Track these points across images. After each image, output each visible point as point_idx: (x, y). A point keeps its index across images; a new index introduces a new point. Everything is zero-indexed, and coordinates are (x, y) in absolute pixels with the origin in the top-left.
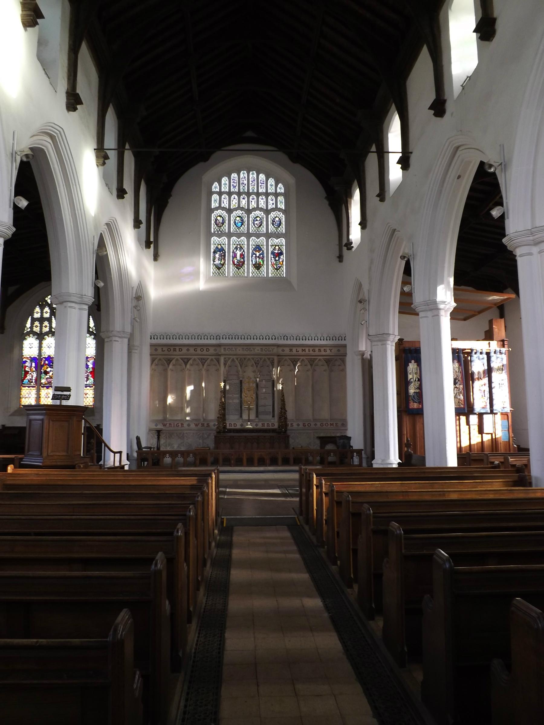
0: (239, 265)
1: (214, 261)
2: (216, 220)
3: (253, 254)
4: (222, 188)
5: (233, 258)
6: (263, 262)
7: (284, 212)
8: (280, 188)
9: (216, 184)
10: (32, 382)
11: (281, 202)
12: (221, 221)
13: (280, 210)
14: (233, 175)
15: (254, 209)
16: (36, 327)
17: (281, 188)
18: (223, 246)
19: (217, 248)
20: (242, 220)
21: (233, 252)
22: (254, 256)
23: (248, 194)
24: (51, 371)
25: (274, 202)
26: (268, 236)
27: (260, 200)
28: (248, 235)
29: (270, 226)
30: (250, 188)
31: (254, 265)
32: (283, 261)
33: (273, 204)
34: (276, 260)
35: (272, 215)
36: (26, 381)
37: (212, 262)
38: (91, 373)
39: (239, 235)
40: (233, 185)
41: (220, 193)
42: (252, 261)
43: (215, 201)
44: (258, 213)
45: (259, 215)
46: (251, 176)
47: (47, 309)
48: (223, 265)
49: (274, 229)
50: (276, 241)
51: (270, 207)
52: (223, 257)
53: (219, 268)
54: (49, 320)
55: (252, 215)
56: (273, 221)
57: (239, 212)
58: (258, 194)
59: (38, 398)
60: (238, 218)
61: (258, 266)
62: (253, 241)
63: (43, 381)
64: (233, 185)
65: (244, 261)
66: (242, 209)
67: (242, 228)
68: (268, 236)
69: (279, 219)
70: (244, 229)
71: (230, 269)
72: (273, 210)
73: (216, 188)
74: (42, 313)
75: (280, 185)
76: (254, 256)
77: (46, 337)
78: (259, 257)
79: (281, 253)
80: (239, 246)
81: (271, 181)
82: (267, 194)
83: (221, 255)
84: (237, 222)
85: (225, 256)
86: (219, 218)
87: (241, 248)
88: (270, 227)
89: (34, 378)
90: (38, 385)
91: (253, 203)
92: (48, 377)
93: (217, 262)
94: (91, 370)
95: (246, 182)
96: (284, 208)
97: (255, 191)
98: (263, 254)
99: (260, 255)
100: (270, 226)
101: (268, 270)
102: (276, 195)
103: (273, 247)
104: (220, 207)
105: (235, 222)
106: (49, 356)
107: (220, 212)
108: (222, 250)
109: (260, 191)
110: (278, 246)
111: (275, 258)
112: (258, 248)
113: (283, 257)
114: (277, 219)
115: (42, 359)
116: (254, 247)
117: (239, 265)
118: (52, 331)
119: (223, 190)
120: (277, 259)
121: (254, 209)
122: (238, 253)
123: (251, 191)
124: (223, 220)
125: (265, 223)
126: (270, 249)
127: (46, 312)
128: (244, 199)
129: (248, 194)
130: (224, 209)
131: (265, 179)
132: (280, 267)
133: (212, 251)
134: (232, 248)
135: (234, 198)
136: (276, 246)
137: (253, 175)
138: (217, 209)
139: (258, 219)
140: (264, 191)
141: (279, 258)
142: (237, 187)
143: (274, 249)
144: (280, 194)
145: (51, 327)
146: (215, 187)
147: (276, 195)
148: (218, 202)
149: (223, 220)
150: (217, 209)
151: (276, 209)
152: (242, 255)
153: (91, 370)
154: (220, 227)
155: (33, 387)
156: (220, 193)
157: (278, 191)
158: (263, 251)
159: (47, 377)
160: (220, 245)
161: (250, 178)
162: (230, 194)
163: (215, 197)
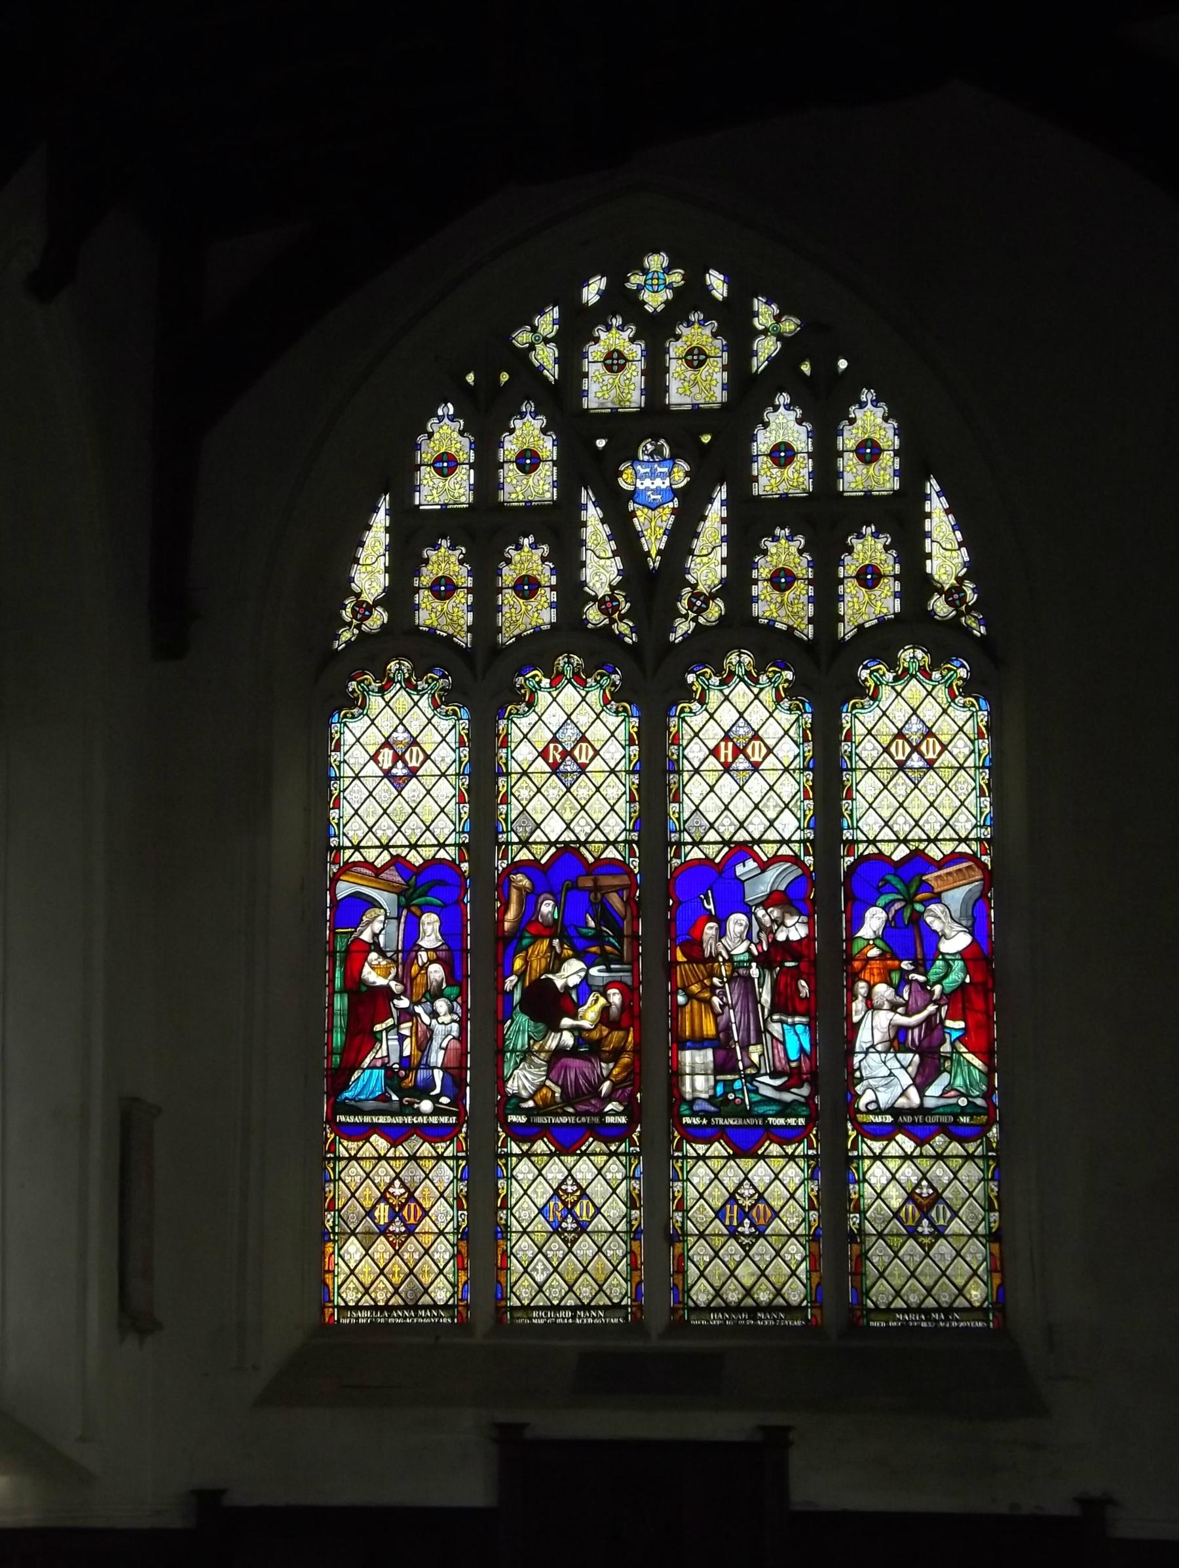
10: (424, 1090)
16: (444, 589)
24: (586, 987)
36: (367, 1082)
38: (958, 1000)
47: (528, 431)
54: (556, 527)
59: (483, 1236)
63: (523, 1080)
74: (487, 469)
89: (437, 1057)
90: (484, 1125)
92: (568, 1039)
94: (957, 975)
106: (568, 852)
115: (504, 884)
153: (957, 975)
155: (432, 1134)
159: (552, 1043)
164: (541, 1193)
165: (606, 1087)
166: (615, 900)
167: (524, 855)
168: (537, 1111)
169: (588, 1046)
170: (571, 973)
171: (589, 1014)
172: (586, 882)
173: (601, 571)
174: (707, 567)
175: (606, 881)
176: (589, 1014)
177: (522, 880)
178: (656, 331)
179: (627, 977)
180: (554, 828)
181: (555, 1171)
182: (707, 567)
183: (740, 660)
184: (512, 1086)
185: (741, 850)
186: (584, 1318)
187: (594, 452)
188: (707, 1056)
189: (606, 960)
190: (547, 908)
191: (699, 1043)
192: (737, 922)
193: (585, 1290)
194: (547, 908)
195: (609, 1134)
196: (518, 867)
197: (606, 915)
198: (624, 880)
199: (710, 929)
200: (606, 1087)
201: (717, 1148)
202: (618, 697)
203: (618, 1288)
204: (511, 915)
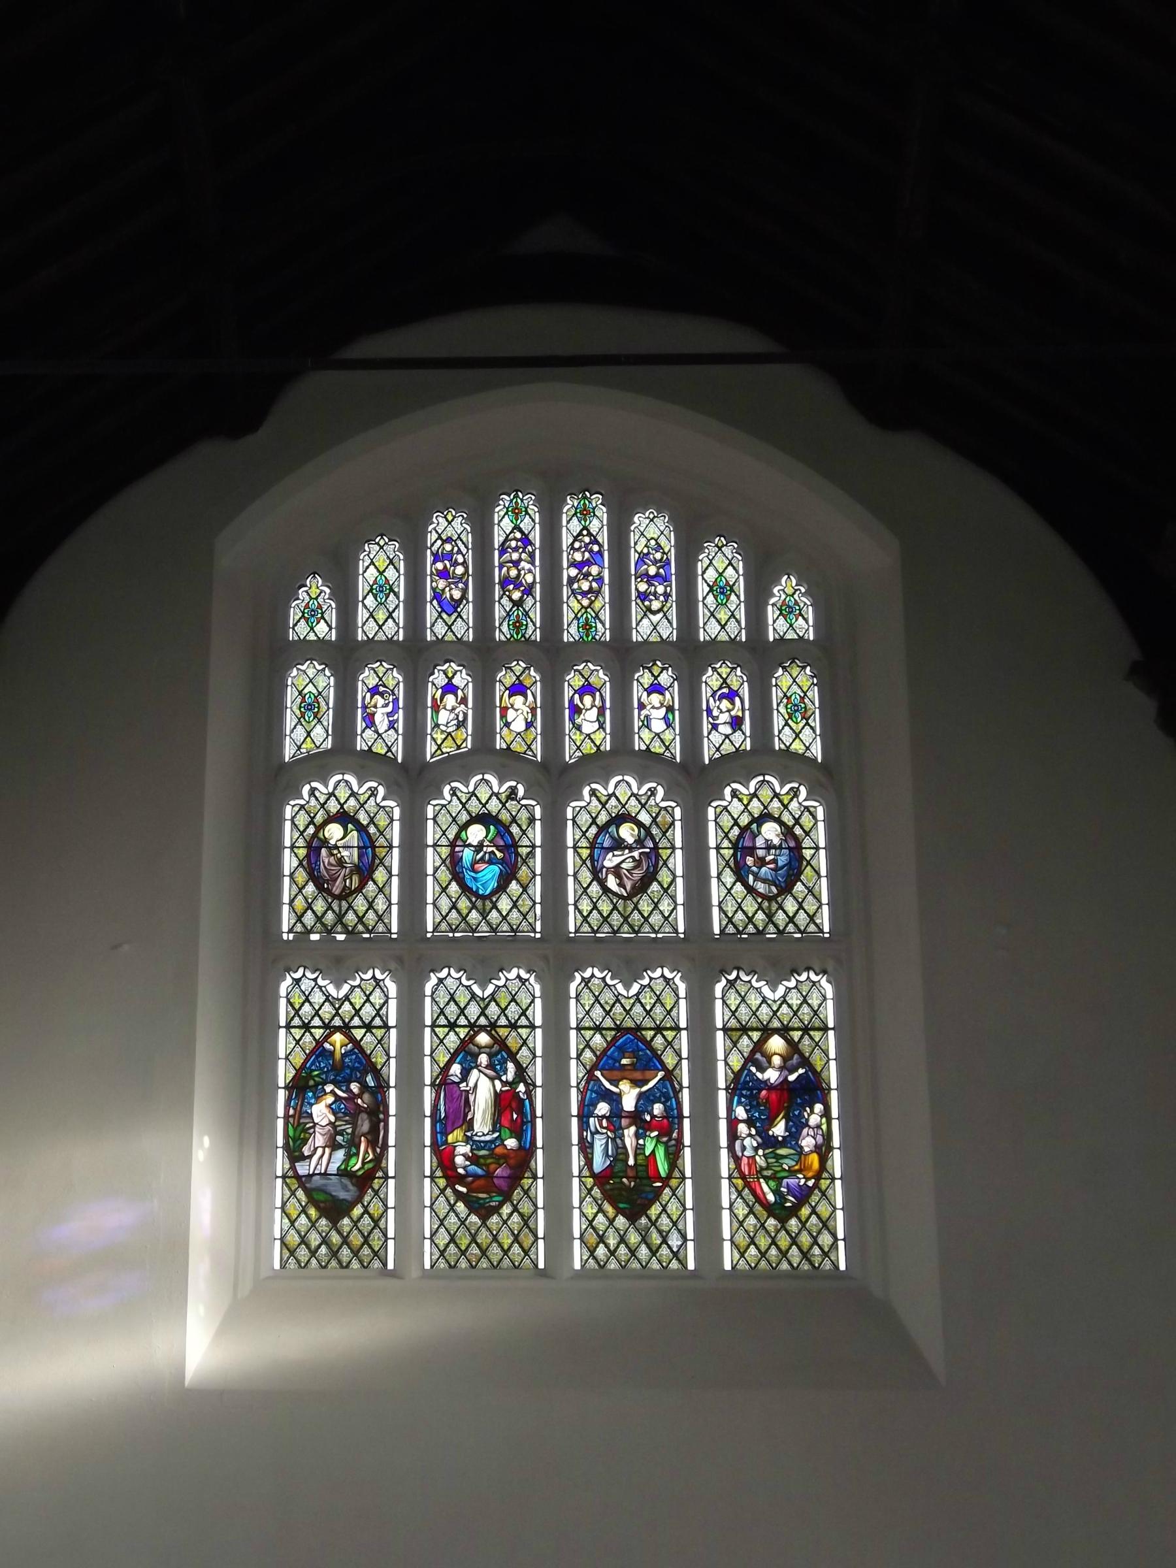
0: (489, 1183)
1: (295, 1154)
2: (316, 845)
3: (593, 1093)
4: (362, 614)
5: (442, 1126)
6: (674, 1157)
7: (823, 777)
8: (787, 610)
9: (316, 589)
11: (797, 710)
12: (350, 856)
13: (790, 764)
14: (439, 523)
15: (598, 765)
17: (791, 612)
18: (368, 1041)
19: (319, 1051)
20: (511, 847)
21: (442, 1082)
22: (603, 1108)
23: (553, 656)
25: (742, 705)
26: (706, 955)
27: (637, 692)
28: (557, 956)
29: (721, 887)
30: (567, 616)
31: (601, 1179)
32: (824, 1150)
33: (736, 723)
34: (769, 1142)
35: (730, 807)
37: (281, 1163)
39: (483, 955)
40: (438, 596)
41: (345, 656)
42: (586, 1148)
43: (310, 707)
44: (624, 788)
45: (633, 806)
46: (570, 527)
48: (364, 1181)
49: (750, 906)
50: (764, 996)
51: (717, 741)
52: (365, 1119)
53: (334, 1210)
55: (584, 810)
56: (742, 848)
57: (487, 788)
58: (624, 656)
60: (476, 833)
61: (630, 1190)
62: (593, 997)
64: (438, 596)
65: (526, 1153)
66: (508, 762)
67: (504, 904)
68: (706, 955)
69: (788, 832)
70: (519, 908)
71: (416, 1211)
72: (736, 765)
73: (312, 614)
75: (786, 587)
76: (603, 1108)
78: (636, 1117)
79: (810, 1089)
80: (483, 1039)
81: (720, 563)
82: (689, 655)
83: (346, 1110)
84: (467, 855)
85: (378, 1112)
86: (334, 832)
87: (502, 1052)
88: (716, 893)
91: (589, 721)
93: (322, 1160)
95: (532, 574)
96: (817, 751)
97: (603, 631)
98: (668, 1091)
99: (645, 1099)
100: (721, 887)
101: (713, 1224)
102: (759, 656)
103: (745, 1043)
104: (343, 754)
105: (454, 862)
107: (343, 787)
108: (360, 1065)
109: (642, 630)
110: (784, 1031)
111: (760, 1125)
112: (630, 1050)
113: (825, 1120)
114: (770, 831)
116: (598, 1040)
117: (489, 1183)
119: (366, 629)
120: (779, 1129)
121: (598, 765)
122: (483, 1090)
123: (571, 633)
124: (368, 844)
125: (678, 862)
126: (727, 1060)
128: (518, 689)
129: (553, 656)
130: (370, 764)
131: (669, 544)
132: (803, 1196)
133: (284, 1074)
134: (436, 1047)
135: (450, 688)
136: (767, 1032)
137: (585, 522)
138: (318, 765)
139: (627, 832)
140: (668, 631)
141: (797, 1126)
142: (468, 611)
143: (757, 1057)
144: (789, 652)
146: (311, 612)
147: (759, 656)
148: (329, 718)
149: (368, 844)
150: (318, 765)
151: (763, 757)
152: (508, 1105)
154: (346, 895)
156: (345, 656)
157: (776, 626)
158: (670, 1076)
160: (346, 1029)
161: (566, 540)
162: (415, 655)
163: (310, 679)
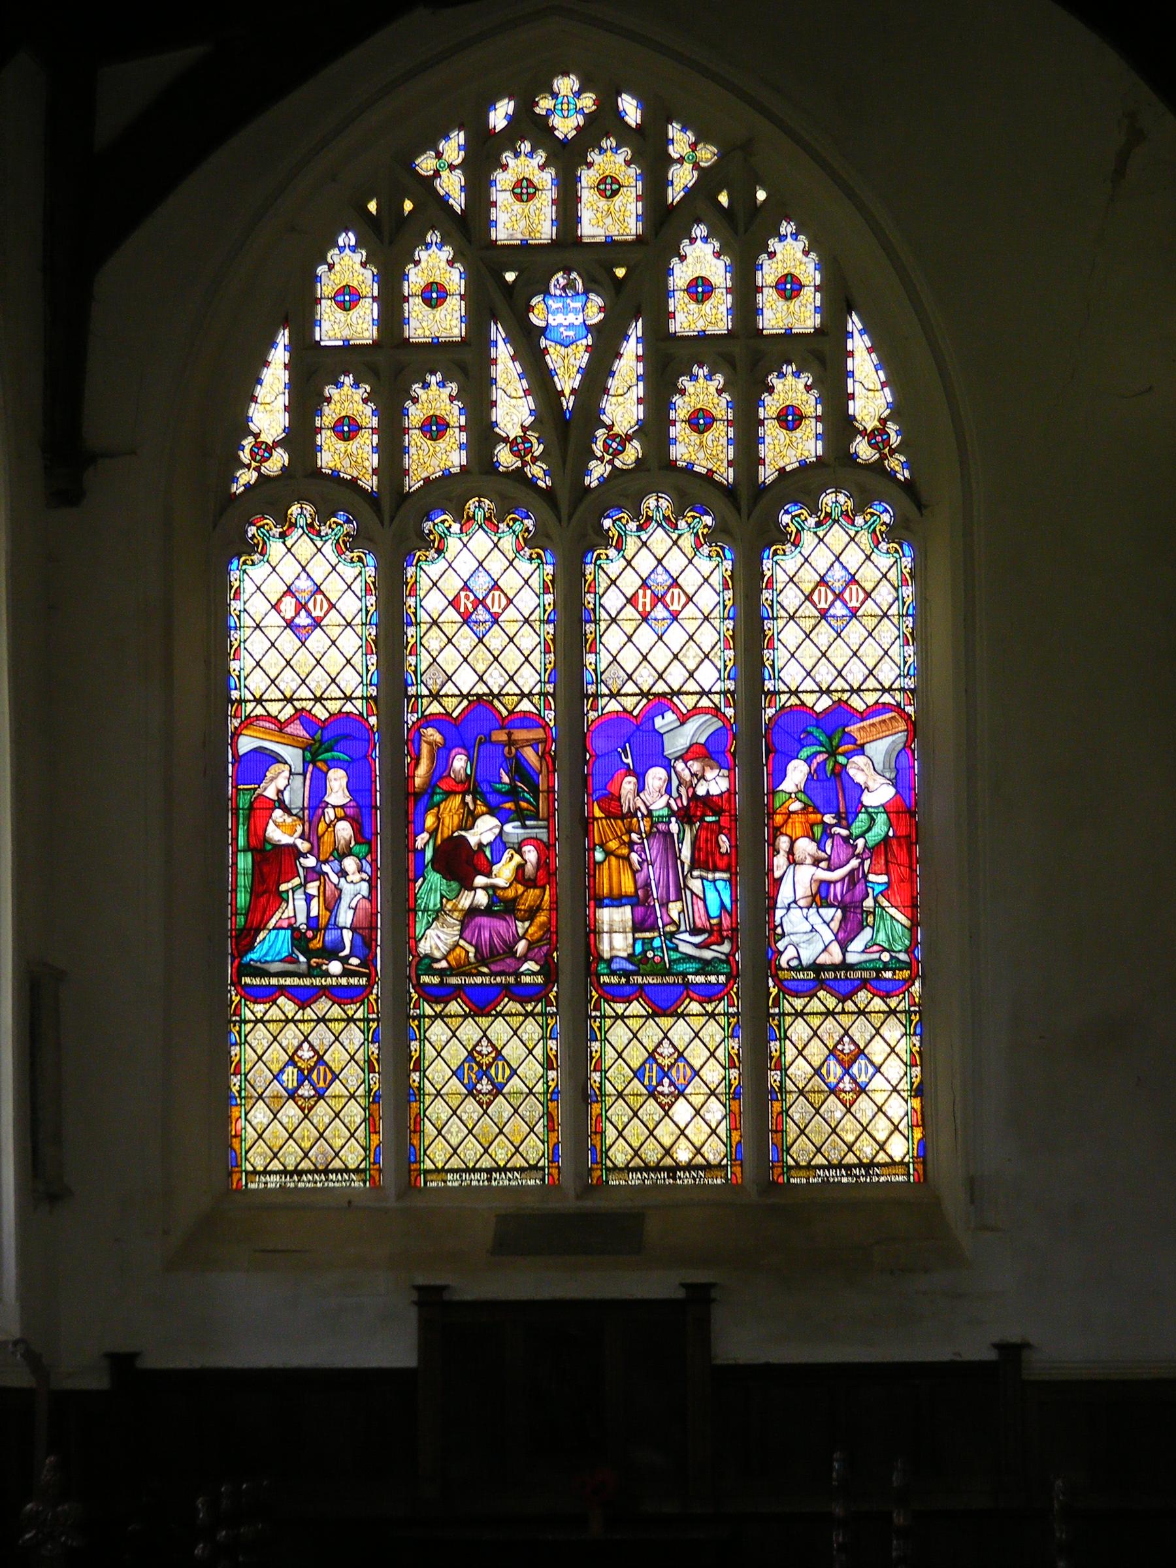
10: (332, 952)
24: (500, 844)
36: (272, 945)
47: (434, 263)
54: (466, 365)
59: (397, 1101)
63: (436, 940)
77: (443, 521)
89: (345, 917)
90: (396, 987)
92: (482, 898)
94: (881, 828)
106: (480, 703)
115: (416, 739)
118: (491, 466)
127: (434, 295)
145: (483, 434)
153: (881, 828)
155: (340, 995)
159: (465, 901)
164: (456, 1054)
165: (521, 946)
166: (530, 754)
167: (435, 708)
168: (452, 971)
169: (502, 906)
170: (484, 830)
171: (504, 873)
172: (500, 736)
173: (513, 411)
174: (623, 408)
175: (520, 735)
176: (504, 873)
177: (432, 734)
178: (567, 158)
179: (543, 834)
180: (466, 680)
181: (469, 1031)
182: (623, 408)
183: (657, 504)
184: (424, 947)
185: (661, 701)
186: (500, 1180)
187: (503, 285)
188: (622, 915)
189: (521, 816)
190: (460, 763)
191: (617, 901)
192: (656, 776)
193: (501, 1153)
194: (460, 763)
195: (523, 994)
196: (428, 721)
197: (520, 770)
198: (539, 734)
199: (629, 785)
200: (521, 946)
201: (636, 1008)
202: (532, 542)
203: (534, 1149)
204: (422, 770)
